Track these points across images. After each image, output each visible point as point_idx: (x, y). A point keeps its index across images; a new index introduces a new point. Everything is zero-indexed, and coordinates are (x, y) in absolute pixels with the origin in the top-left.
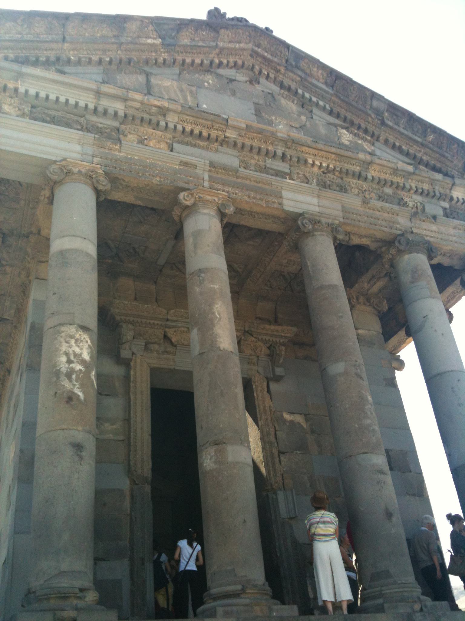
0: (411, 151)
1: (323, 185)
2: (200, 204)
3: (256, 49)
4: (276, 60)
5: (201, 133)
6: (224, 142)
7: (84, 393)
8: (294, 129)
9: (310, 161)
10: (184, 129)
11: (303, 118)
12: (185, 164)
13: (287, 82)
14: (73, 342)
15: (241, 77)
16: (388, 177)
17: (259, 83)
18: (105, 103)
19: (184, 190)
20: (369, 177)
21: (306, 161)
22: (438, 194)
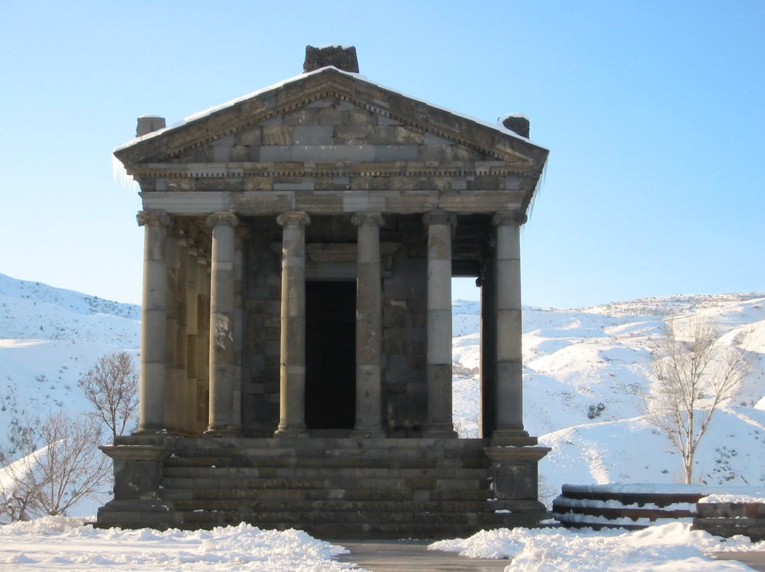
0: (452, 136)
1: (373, 189)
2: (288, 222)
3: (333, 85)
4: (348, 90)
5: (289, 173)
6: (305, 175)
7: (226, 347)
8: (361, 140)
9: (363, 174)
10: (279, 173)
11: (370, 127)
12: (281, 196)
13: (358, 101)
14: (220, 322)
15: (327, 104)
16: (423, 170)
17: (339, 104)
18: (232, 171)
19: (279, 214)
20: (407, 174)
21: (360, 174)
22: (463, 174)
